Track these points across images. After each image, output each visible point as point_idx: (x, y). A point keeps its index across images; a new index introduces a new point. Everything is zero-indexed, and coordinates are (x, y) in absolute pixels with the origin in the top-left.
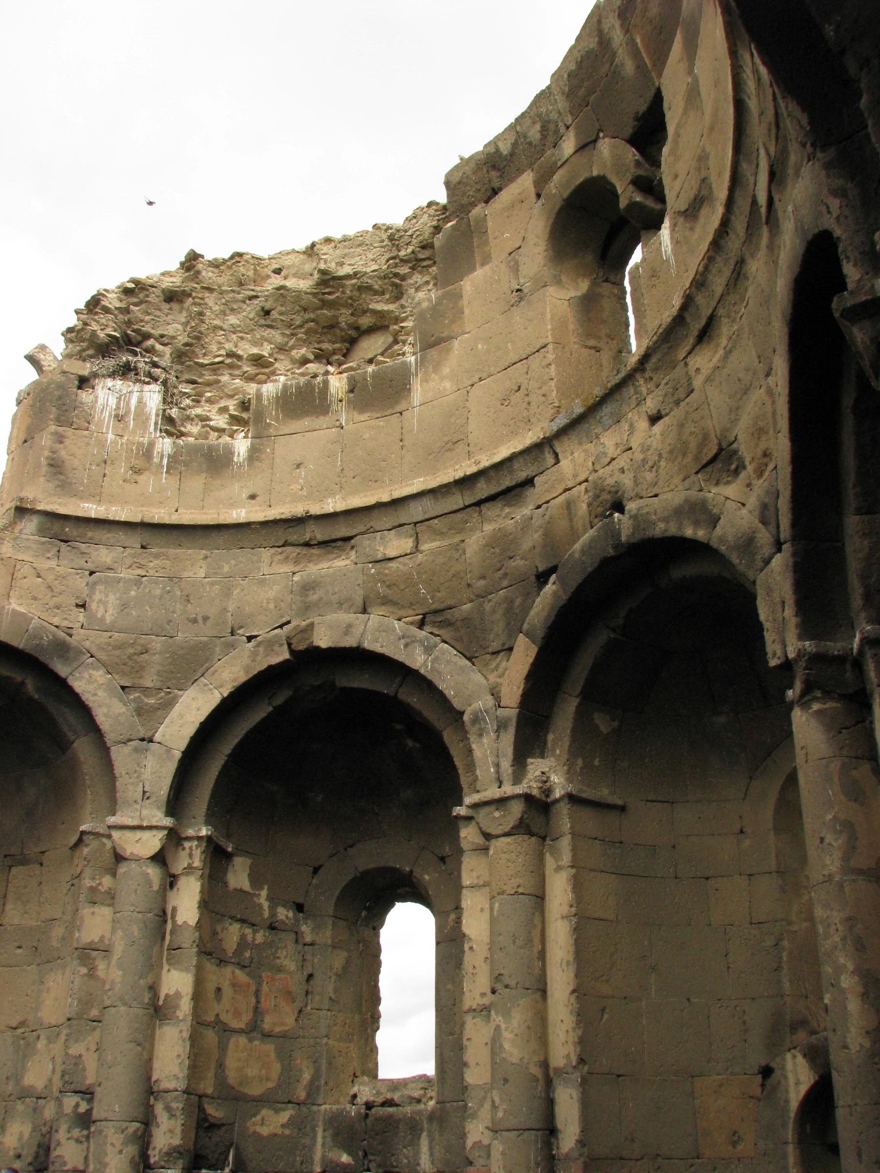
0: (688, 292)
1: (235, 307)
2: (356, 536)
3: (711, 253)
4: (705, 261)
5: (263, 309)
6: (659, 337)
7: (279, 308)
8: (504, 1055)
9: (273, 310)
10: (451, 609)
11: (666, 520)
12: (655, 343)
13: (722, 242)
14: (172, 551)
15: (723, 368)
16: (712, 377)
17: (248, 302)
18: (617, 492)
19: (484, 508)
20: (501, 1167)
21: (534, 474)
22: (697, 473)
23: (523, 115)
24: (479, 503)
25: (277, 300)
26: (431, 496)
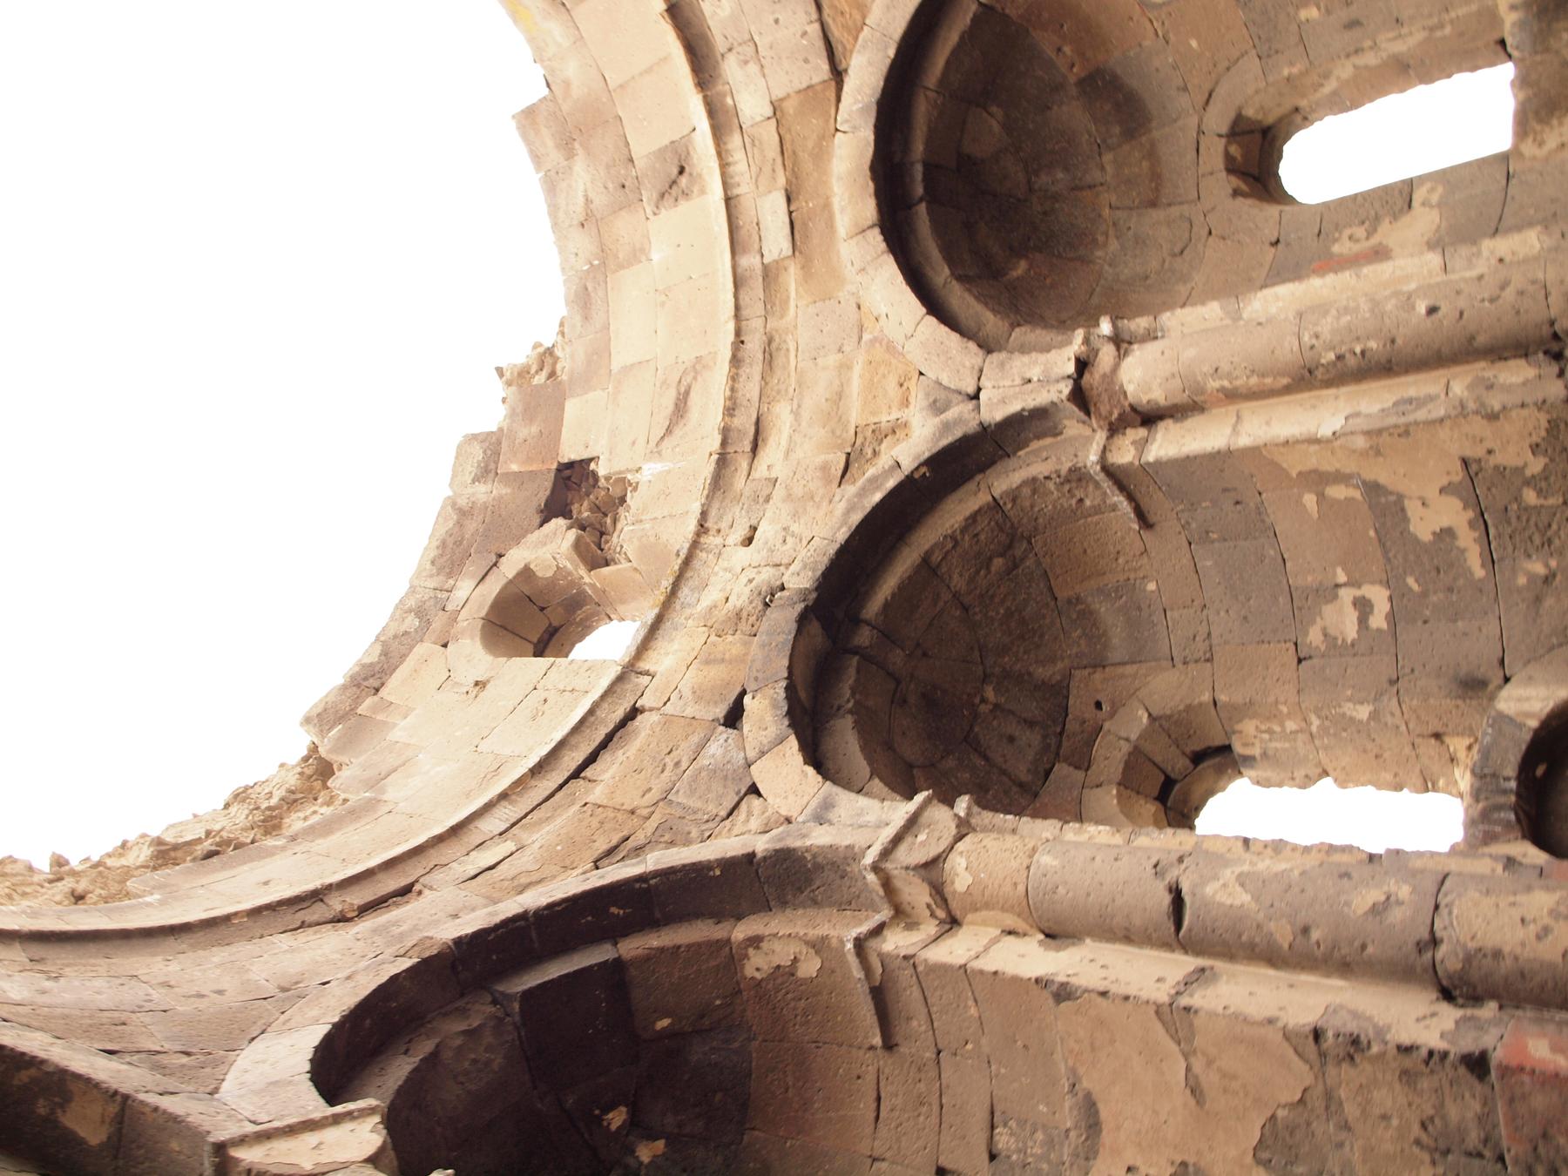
0: (722, 425)
1: (28, 890)
2: (417, 881)
3: (733, 370)
4: (730, 382)
5: (73, 893)
6: (709, 489)
7: (99, 891)
8: (1296, 873)
9: (91, 893)
10: (627, 839)
11: (844, 523)
12: (708, 496)
13: (740, 355)
14: (92, 961)
15: (799, 425)
16: (792, 445)
17: (47, 885)
18: (760, 594)
19: (588, 773)
20: (1512, 899)
21: (633, 703)
22: (839, 486)
23: (454, 465)
24: (576, 774)
25: (94, 881)
26: (504, 803)
